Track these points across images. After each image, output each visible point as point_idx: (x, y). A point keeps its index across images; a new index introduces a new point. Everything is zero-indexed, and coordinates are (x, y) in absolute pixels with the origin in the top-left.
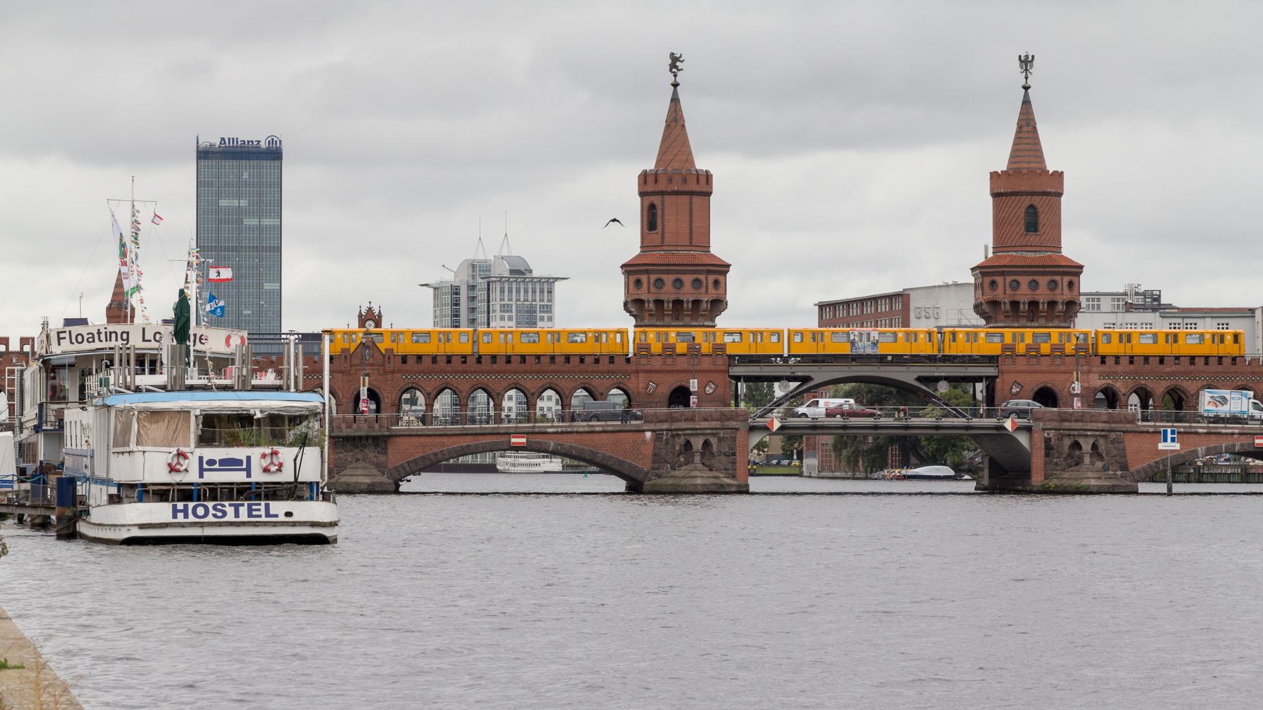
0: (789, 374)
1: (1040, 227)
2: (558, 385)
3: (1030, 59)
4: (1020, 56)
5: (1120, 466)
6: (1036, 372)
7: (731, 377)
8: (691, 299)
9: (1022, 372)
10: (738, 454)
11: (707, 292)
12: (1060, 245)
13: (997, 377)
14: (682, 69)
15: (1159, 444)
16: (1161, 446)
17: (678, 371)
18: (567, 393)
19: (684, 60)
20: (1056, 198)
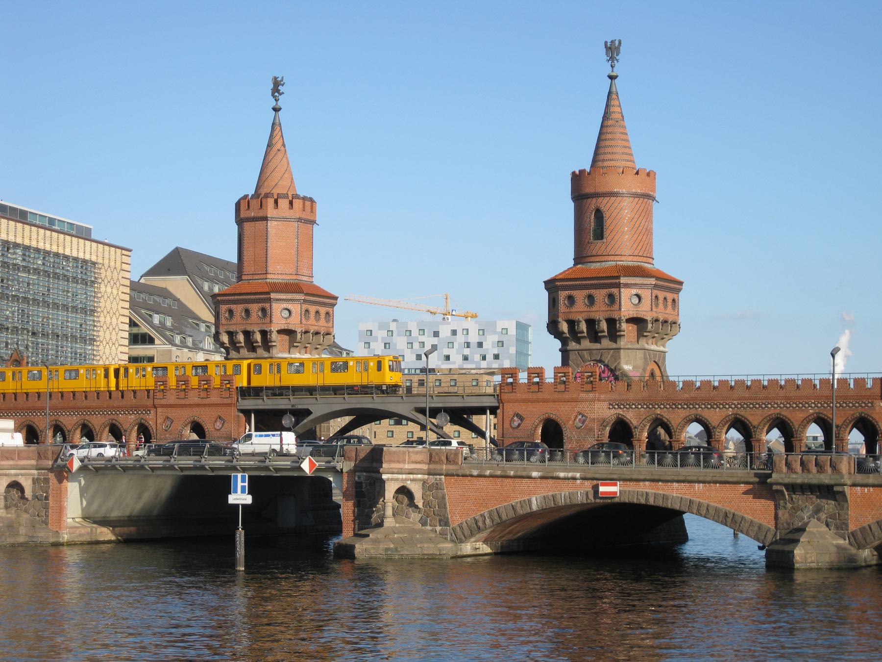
0: (290, 407)
1: (606, 234)
2: (89, 422)
3: (617, 43)
4: (606, 43)
5: (440, 521)
6: (538, 401)
7: (242, 411)
8: (256, 329)
9: (525, 401)
10: (50, 498)
11: (271, 322)
12: (651, 252)
13: (498, 408)
14: (283, 93)
15: (230, 496)
16: (232, 499)
17: (190, 406)
18: (97, 430)
19: (284, 83)
20: (646, 200)
